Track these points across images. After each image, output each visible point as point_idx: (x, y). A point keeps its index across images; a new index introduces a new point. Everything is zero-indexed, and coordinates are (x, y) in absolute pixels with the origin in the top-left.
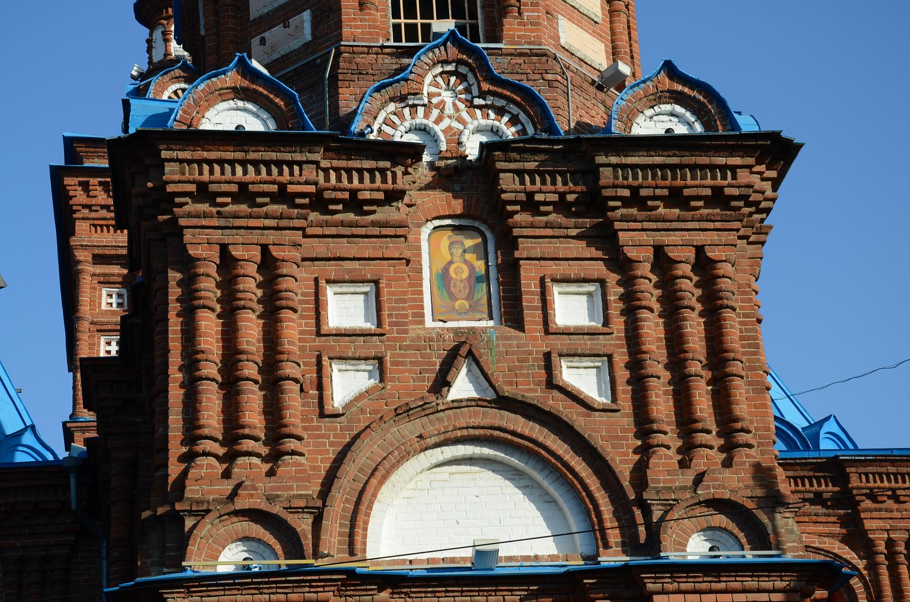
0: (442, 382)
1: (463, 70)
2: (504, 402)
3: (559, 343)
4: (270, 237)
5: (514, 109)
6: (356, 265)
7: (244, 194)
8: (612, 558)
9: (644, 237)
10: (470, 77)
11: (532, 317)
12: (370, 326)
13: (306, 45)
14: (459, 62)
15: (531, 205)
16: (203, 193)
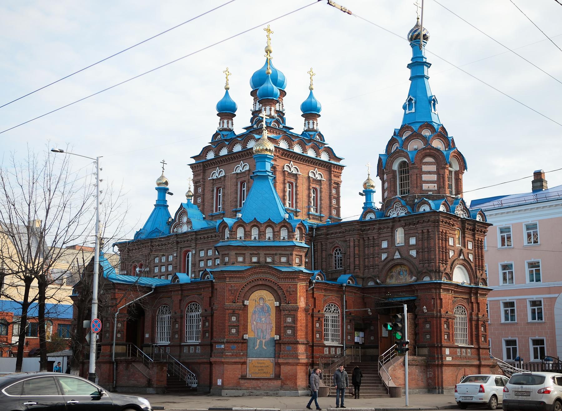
0: (460, 255)
1: (461, 204)
2: (465, 260)
3: (469, 251)
4: (447, 229)
5: (466, 212)
6: (451, 235)
7: (446, 223)
8: (473, 285)
9: (477, 236)
10: (462, 205)
11: (466, 246)
12: (453, 245)
13: (435, 190)
14: (462, 203)
15: (467, 229)
16: (442, 222)
